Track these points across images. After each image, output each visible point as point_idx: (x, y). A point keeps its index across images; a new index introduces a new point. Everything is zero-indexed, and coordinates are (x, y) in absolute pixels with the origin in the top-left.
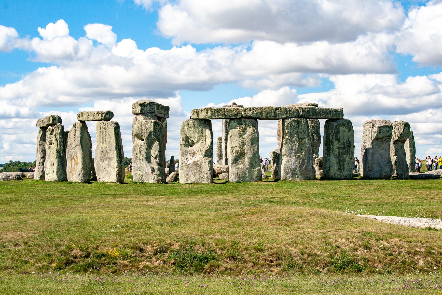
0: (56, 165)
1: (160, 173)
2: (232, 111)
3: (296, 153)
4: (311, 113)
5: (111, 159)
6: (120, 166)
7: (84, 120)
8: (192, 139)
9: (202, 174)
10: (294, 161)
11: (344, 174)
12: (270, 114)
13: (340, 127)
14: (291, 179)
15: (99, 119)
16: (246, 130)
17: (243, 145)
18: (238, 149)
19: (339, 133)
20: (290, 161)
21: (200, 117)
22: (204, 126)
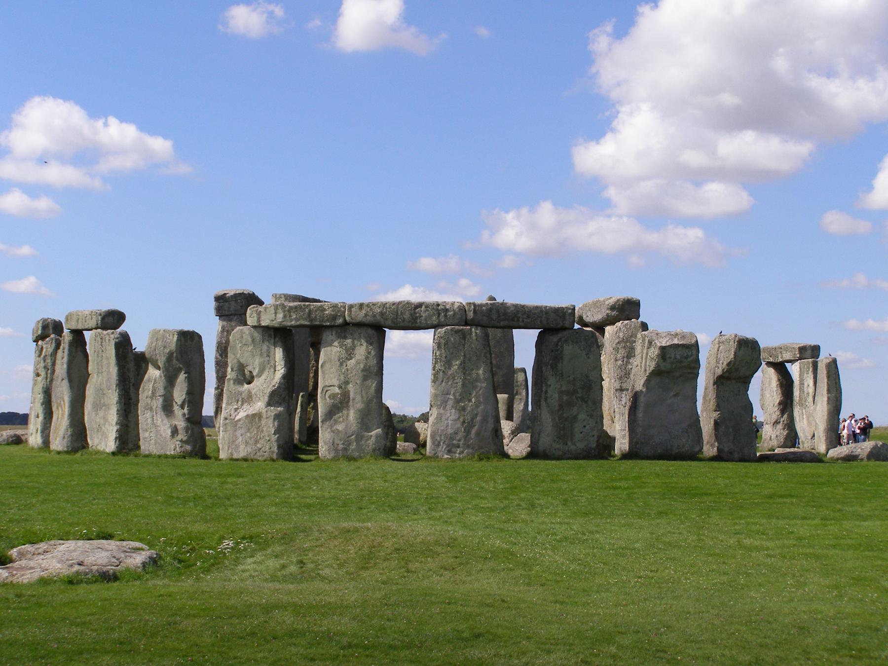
0: (41, 418)
1: (189, 437)
2: (325, 310)
3: (458, 401)
4: (494, 316)
5: (108, 406)
7: (80, 327)
8: (250, 368)
9: (261, 442)
10: (453, 417)
11: (573, 448)
12: (410, 318)
13: (566, 347)
14: (446, 456)
15: (94, 326)
16: (353, 349)
17: (347, 383)
18: (337, 390)
19: (562, 358)
20: (444, 418)
22: (272, 341)
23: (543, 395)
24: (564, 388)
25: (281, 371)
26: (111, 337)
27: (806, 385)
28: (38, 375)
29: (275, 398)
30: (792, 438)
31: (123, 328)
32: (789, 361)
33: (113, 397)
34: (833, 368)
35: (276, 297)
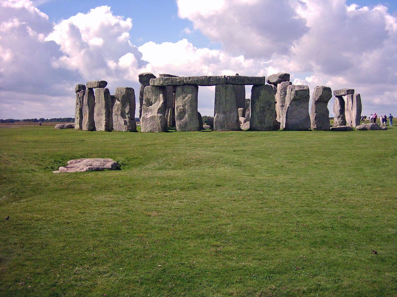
5: (102, 114)
6: (108, 120)
8: (151, 100)
12: (207, 81)
13: (262, 91)
21: (155, 85)
22: (159, 91)
23: (254, 108)
24: (261, 106)
25: (162, 101)
26: (102, 90)
27: (349, 104)
28: (77, 104)
29: (160, 111)
30: (344, 122)
31: (106, 87)
32: (343, 95)
33: (104, 111)
34: (358, 96)
35: (161, 75)
